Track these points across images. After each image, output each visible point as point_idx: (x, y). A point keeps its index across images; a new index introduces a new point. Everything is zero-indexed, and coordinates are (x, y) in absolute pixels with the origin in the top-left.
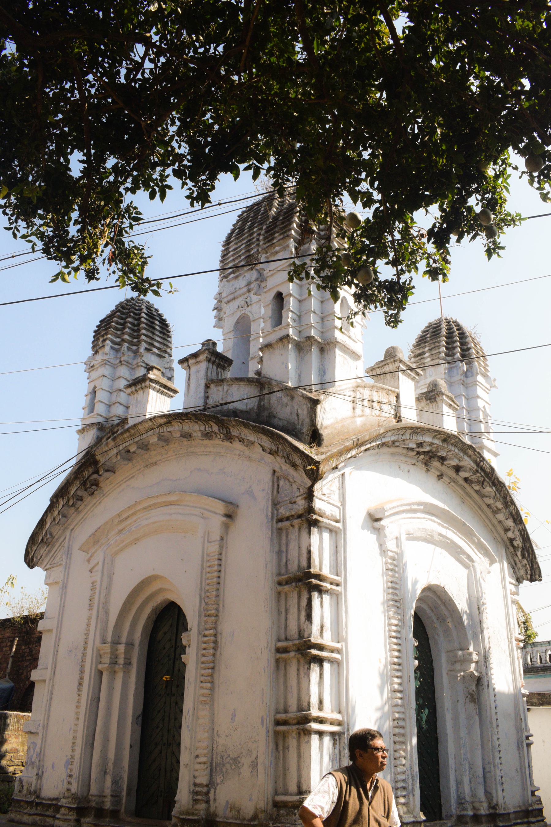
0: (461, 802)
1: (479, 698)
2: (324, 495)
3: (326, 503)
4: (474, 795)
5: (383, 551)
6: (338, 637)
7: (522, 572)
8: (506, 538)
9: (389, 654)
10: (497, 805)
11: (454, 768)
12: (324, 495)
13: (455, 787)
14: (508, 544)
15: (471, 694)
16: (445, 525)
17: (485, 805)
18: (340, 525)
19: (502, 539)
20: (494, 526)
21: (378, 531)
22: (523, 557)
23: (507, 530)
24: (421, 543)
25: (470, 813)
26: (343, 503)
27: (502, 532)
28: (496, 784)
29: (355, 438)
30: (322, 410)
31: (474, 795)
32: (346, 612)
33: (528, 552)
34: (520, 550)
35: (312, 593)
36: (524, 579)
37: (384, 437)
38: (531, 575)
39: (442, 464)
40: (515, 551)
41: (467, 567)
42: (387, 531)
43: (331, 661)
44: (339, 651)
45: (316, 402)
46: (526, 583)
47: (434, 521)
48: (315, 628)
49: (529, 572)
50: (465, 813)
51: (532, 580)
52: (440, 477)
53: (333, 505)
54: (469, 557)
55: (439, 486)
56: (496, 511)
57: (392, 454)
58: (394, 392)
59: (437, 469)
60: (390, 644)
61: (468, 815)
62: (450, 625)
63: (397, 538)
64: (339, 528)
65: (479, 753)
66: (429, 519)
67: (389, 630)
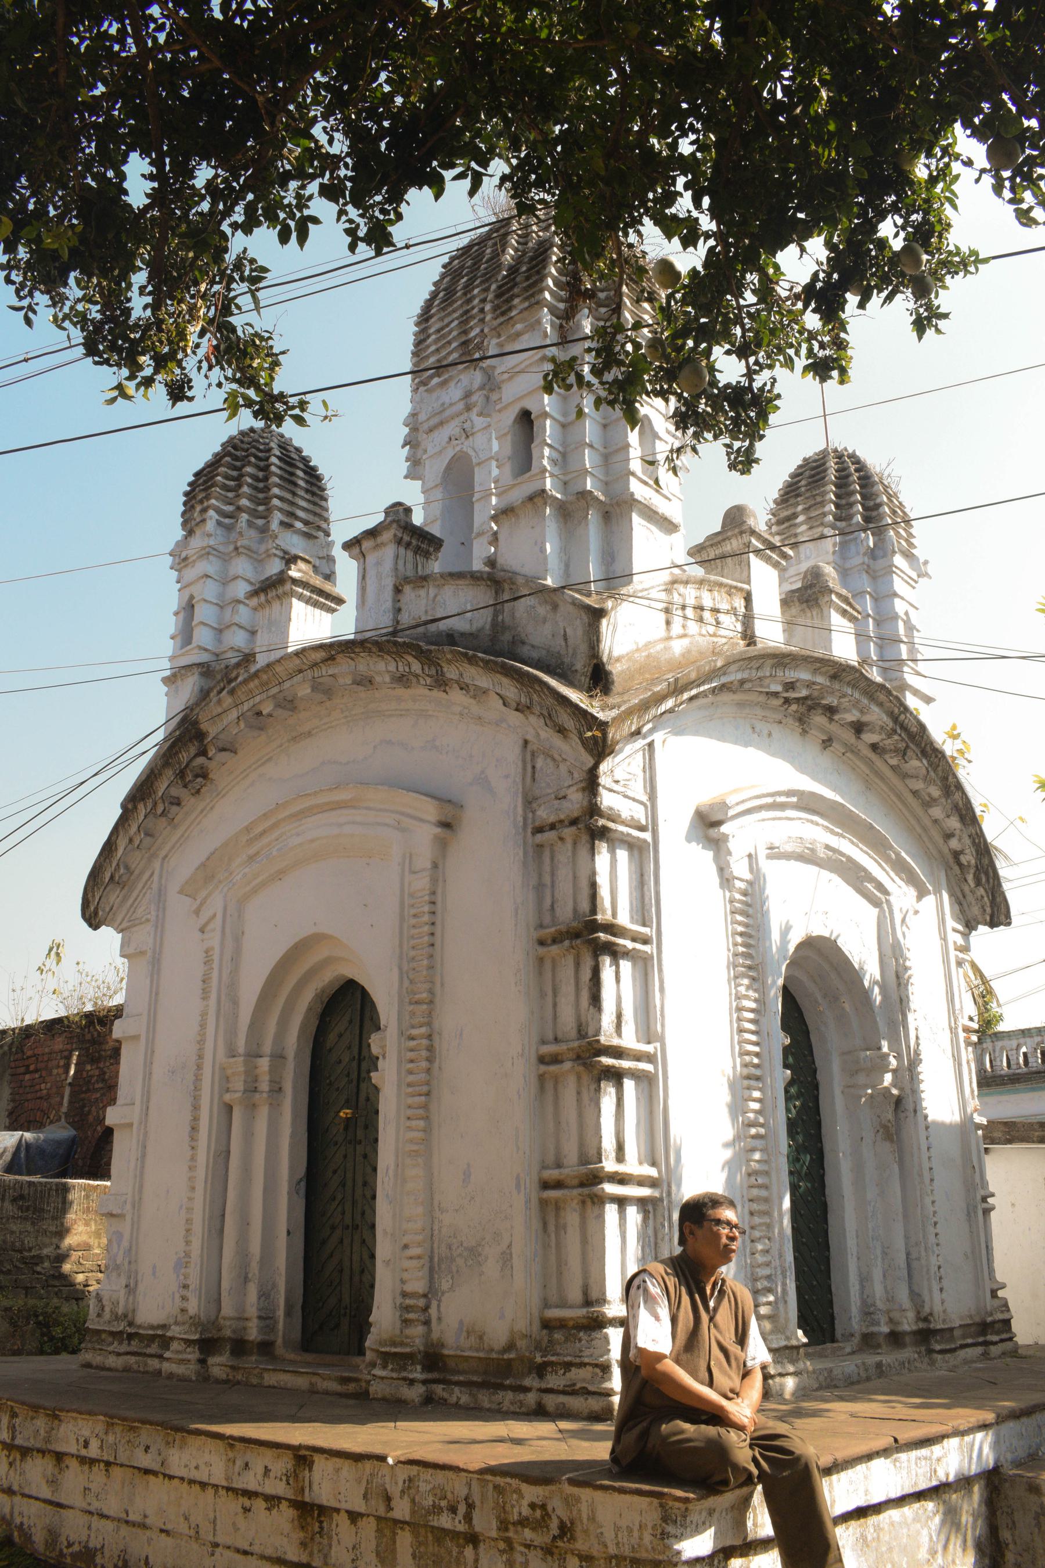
0: (868, 1312)
1: (898, 1131)
2: (617, 782)
3: (620, 796)
4: (890, 1299)
5: (726, 880)
6: (648, 1031)
7: (976, 910)
8: (946, 851)
10: (931, 1314)
12: (617, 782)
13: (857, 1287)
14: (951, 860)
15: (885, 1127)
17: (911, 1315)
18: (647, 836)
19: (940, 852)
20: (925, 829)
21: (717, 845)
22: (978, 883)
23: (948, 836)
25: (885, 1329)
27: (941, 841)
28: (929, 1279)
29: (670, 677)
30: (611, 627)
31: (890, 1299)
32: (662, 990)
33: (987, 874)
34: (972, 871)
35: (600, 958)
36: (979, 923)
37: (724, 674)
38: (992, 916)
39: (831, 720)
40: (962, 873)
41: (876, 903)
42: (732, 845)
43: (638, 1076)
44: (650, 1058)
45: (598, 614)
46: (982, 929)
47: (817, 824)
48: (607, 1020)
49: (988, 910)
50: (875, 1329)
51: (993, 924)
52: (827, 743)
53: (634, 800)
54: (880, 887)
55: (825, 760)
56: (928, 803)
57: (741, 705)
58: (741, 590)
59: (823, 730)
60: (739, 1043)
61: (880, 1333)
62: (847, 1006)
63: (750, 856)
64: (645, 841)
65: (899, 1229)
66: (808, 821)
67: (739, 1019)
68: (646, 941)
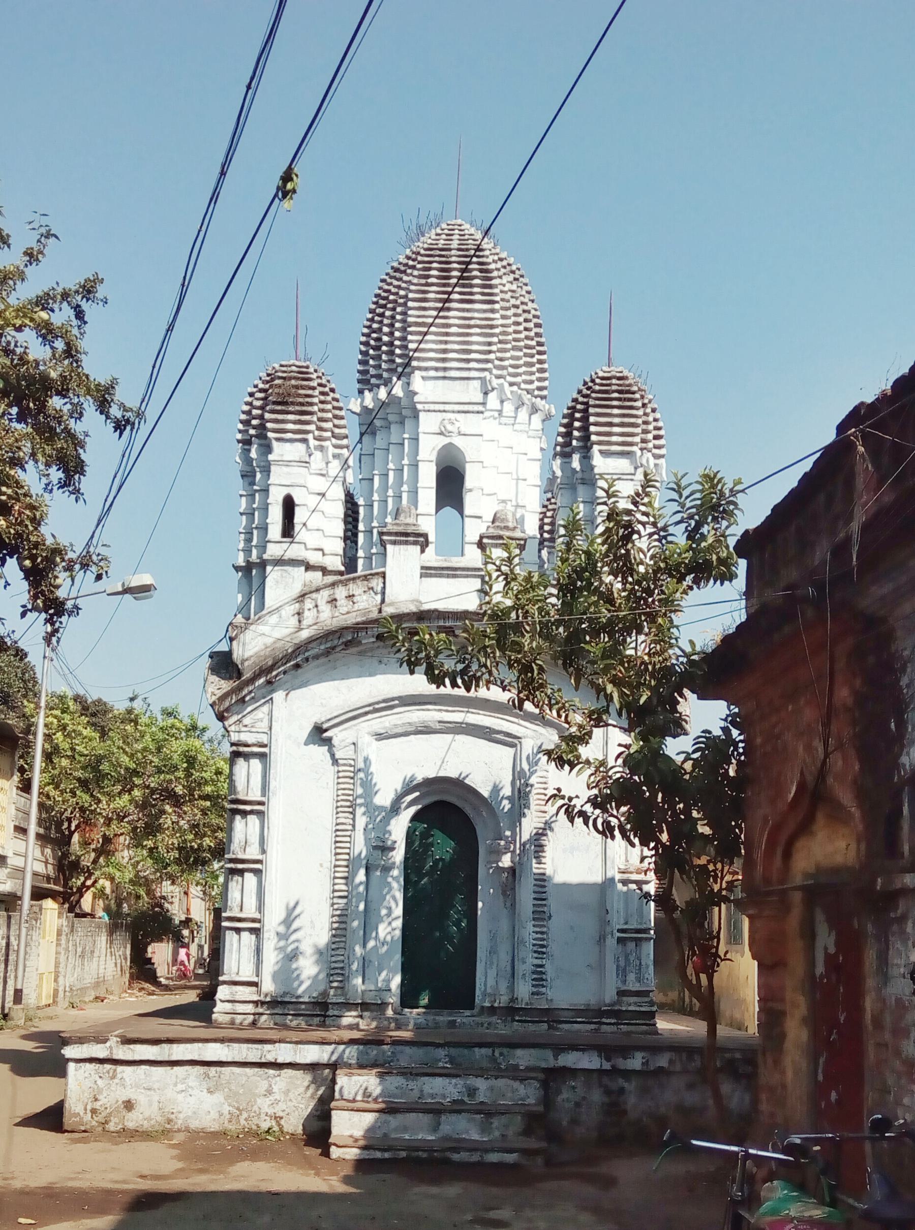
0: (485, 994)
1: (513, 889)
2: (246, 726)
5: (335, 761)
9: (334, 858)
11: (484, 960)
12: (246, 726)
16: (450, 709)
21: (328, 742)
24: (412, 736)
25: (487, 1004)
26: (271, 729)
30: (241, 644)
37: (307, 651)
42: (335, 741)
47: (429, 710)
57: (360, 653)
58: (377, 574)
63: (354, 744)
68: (261, 803)
